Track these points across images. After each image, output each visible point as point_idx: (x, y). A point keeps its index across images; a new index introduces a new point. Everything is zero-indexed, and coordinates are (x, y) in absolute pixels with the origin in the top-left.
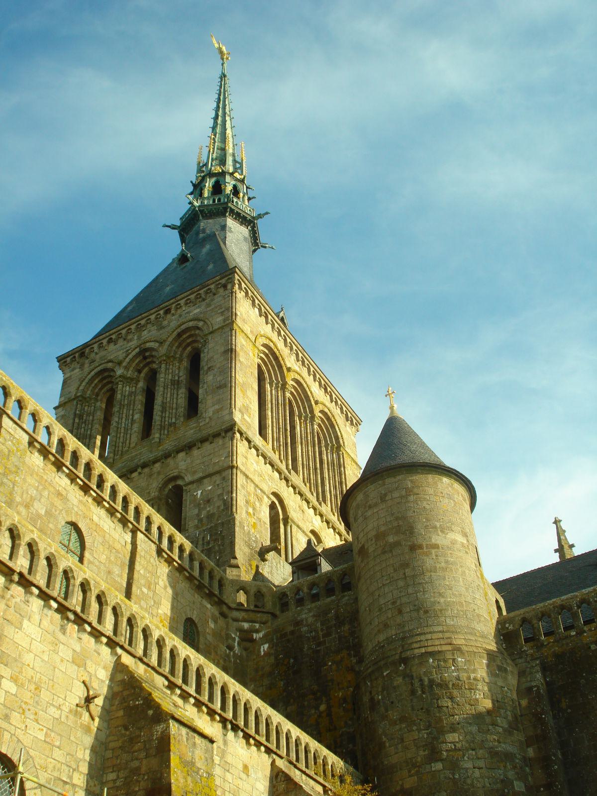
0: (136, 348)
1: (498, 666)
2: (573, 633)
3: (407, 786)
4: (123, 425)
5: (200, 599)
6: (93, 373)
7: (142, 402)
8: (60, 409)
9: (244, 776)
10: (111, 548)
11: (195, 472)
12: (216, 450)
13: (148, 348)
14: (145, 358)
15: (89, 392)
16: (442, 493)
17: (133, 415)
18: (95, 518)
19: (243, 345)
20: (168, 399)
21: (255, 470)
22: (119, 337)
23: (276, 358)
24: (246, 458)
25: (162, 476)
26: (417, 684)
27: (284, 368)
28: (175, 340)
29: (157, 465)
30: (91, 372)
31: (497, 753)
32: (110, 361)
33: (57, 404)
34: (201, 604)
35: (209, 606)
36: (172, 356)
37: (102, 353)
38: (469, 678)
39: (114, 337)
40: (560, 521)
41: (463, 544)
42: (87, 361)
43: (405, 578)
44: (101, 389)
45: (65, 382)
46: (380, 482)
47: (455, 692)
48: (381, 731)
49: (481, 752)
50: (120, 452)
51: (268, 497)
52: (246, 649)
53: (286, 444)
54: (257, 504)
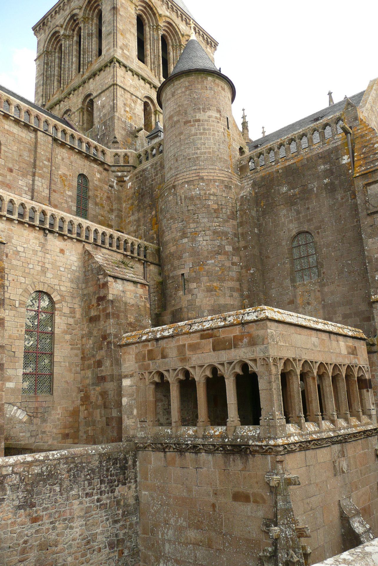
0: (69, 15)
1: (225, 185)
2: (273, 164)
3: (171, 251)
4: (67, 66)
5: (89, 163)
6: (50, 35)
7: (77, 50)
8: (37, 60)
9: (61, 255)
10: (20, 142)
11: (98, 90)
12: (107, 75)
13: (75, 14)
14: (75, 21)
15: (50, 48)
16: (206, 87)
17: (72, 59)
18: (6, 127)
19: (123, 3)
20: (87, 46)
21: (131, 84)
22: (60, 9)
23: (151, 9)
24: (124, 78)
25: (83, 95)
26: (179, 198)
27: (157, 15)
28: (87, 5)
29: (81, 88)
30: (49, 34)
31: (217, 232)
32: (57, 26)
33: (35, 58)
34: (89, 165)
35: (96, 166)
36: (87, 17)
37: (53, 21)
38: (205, 194)
39: (57, 9)
40: (331, 93)
41: (216, 118)
42: (47, 28)
43: (180, 141)
44: (57, 45)
45: (38, 43)
46: (172, 84)
47: (198, 202)
48: (163, 224)
49: (208, 232)
50: (67, 83)
51: (141, 100)
52: (121, 186)
53: (159, 65)
54: (133, 105)
